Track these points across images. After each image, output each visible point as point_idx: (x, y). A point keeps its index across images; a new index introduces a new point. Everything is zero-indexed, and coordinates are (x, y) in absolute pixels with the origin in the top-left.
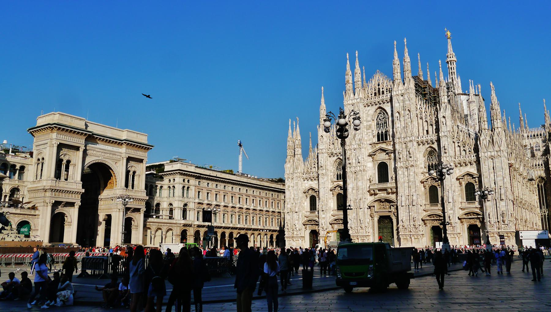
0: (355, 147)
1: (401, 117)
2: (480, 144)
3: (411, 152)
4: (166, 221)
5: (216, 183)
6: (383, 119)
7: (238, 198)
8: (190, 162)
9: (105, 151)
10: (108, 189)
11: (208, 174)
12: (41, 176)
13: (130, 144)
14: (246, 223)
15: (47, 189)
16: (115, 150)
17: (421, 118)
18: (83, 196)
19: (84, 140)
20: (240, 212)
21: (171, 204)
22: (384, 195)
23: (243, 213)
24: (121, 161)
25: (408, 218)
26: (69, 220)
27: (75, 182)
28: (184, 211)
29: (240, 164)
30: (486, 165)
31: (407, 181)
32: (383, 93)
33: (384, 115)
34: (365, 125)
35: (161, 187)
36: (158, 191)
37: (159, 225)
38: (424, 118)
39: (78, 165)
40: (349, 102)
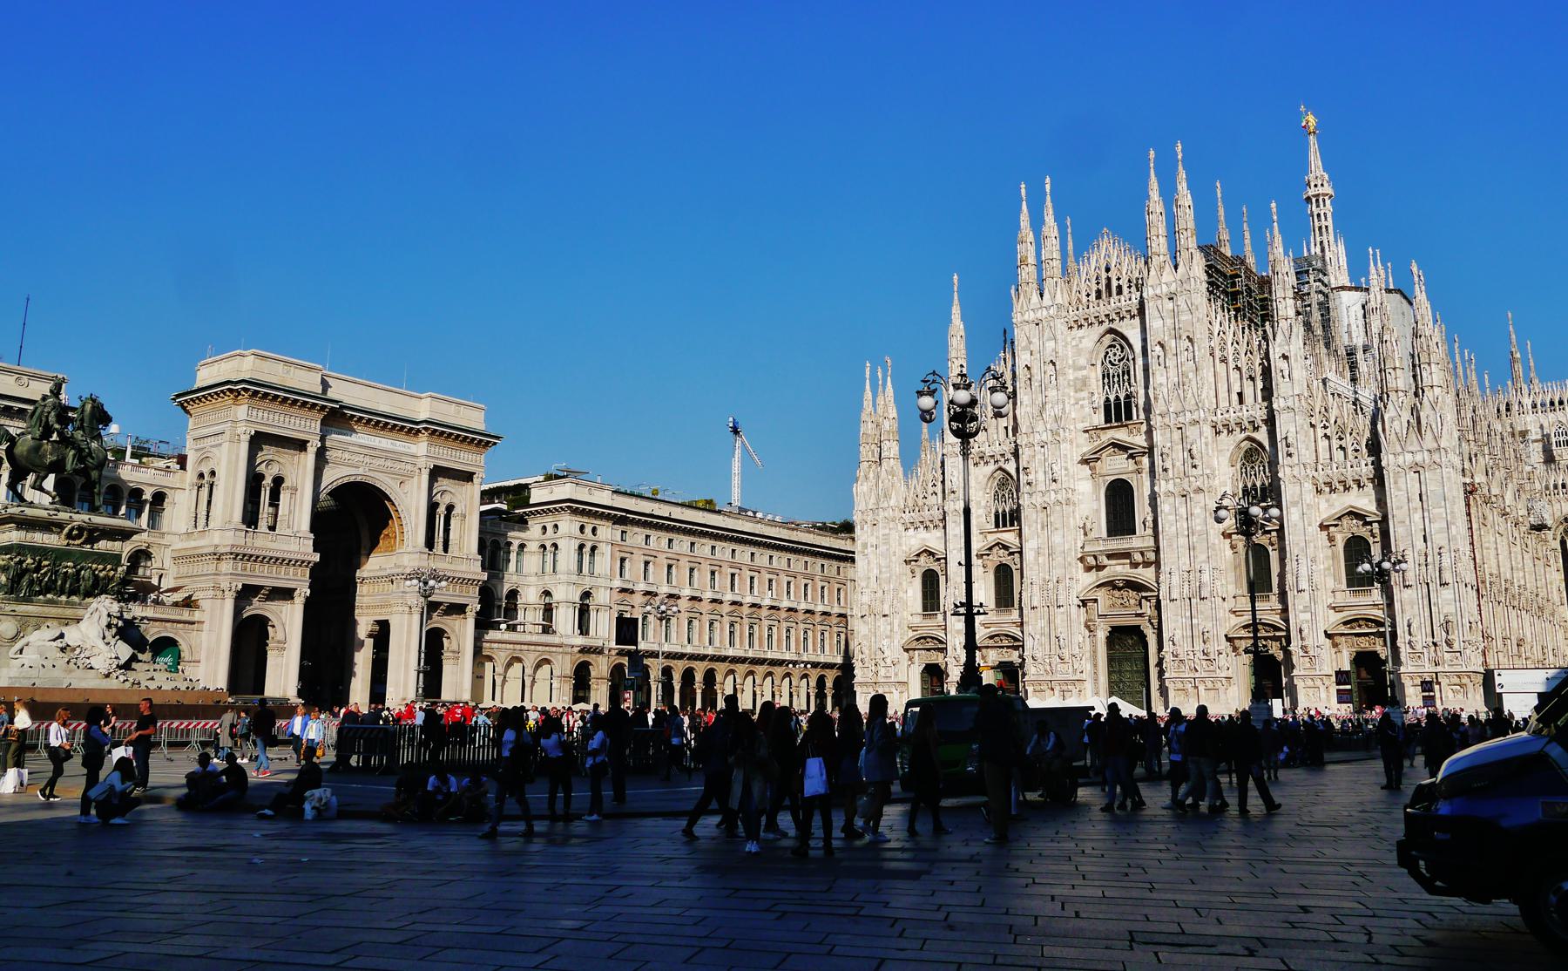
0: (1044, 438)
1: (1169, 356)
2: (1384, 430)
3: (1194, 452)
4: (535, 638)
5: (668, 534)
6: (1119, 361)
7: (729, 577)
8: (599, 480)
10: (381, 552)
11: (648, 511)
12: (207, 519)
13: (440, 432)
14: (751, 645)
15: (222, 554)
16: (399, 448)
17: (1224, 360)
18: (316, 572)
20: (735, 614)
21: (547, 593)
22: (1124, 568)
23: (742, 618)
24: (416, 478)
25: (1189, 633)
26: (280, 636)
27: (295, 536)
28: (584, 612)
29: (736, 481)
30: (1399, 490)
31: (1186, 533)
32: (1119, 288)
33: (1122, 352)
34: (1071, 378)
35: (522, 546)
36: (513, 556)
38: (1230, 359)
39: (303, 489)
40: (1026, 317)
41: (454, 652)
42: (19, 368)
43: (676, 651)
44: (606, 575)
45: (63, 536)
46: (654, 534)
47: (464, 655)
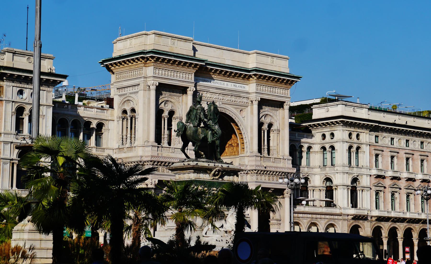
5: (406, 137)
8: (358, 101)
9: (223, 92)
10: (227, 156)
11: (392, 121)
19: (193, 75)
21: (328, 179)
24: (249, 107)
28: (354, 192)
35: (309, 148)
36: (304, 155)
37: (312, 218)
41: (277, 220)
42: (26, 52)
43: (415, 217)
44: (367, 166)
45: (211, 175)
46: (396, 137)
47: (284, 222)
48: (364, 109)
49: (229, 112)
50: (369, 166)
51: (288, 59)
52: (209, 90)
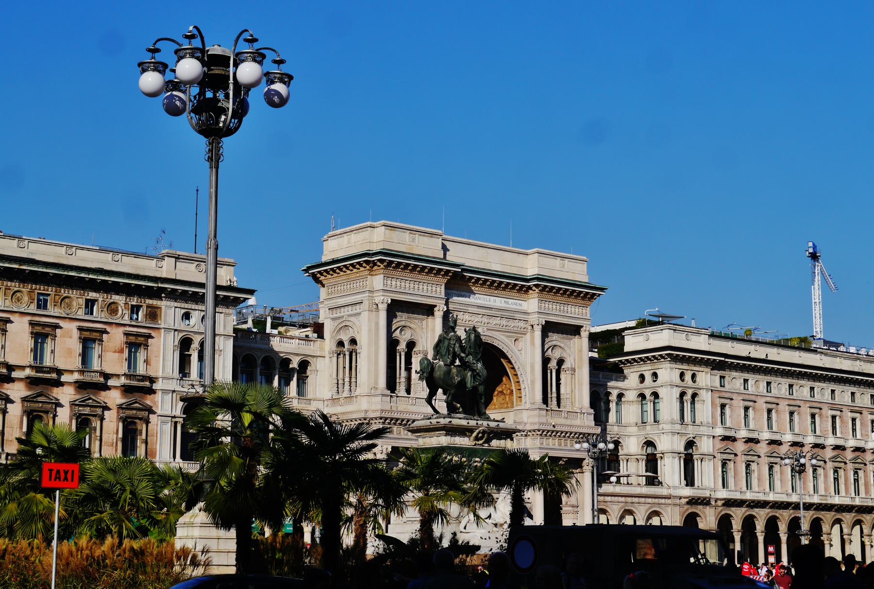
5: (766, 377)
7: (830, 420)
8: (693, 324)
9: (490, 312)
10: (495, 409)
14: (857, 492)
19: (443, 287)
20: (839, 459)
21: (649, 444)
23: (845, 463)
24: (528, 335)
28: (688, 463)
29: (817, 311)
35: (620, 396)
36: (613, 406)
37: (626, 502)
41: (573, 506)
43: (781, 500)
45: (472, 438)
46: (752, 378)
47: (583, 509)
48: (703, 335)
49: (498, 342)
50: (711, 422)
51: (586, 261)
52: (468, 310)
